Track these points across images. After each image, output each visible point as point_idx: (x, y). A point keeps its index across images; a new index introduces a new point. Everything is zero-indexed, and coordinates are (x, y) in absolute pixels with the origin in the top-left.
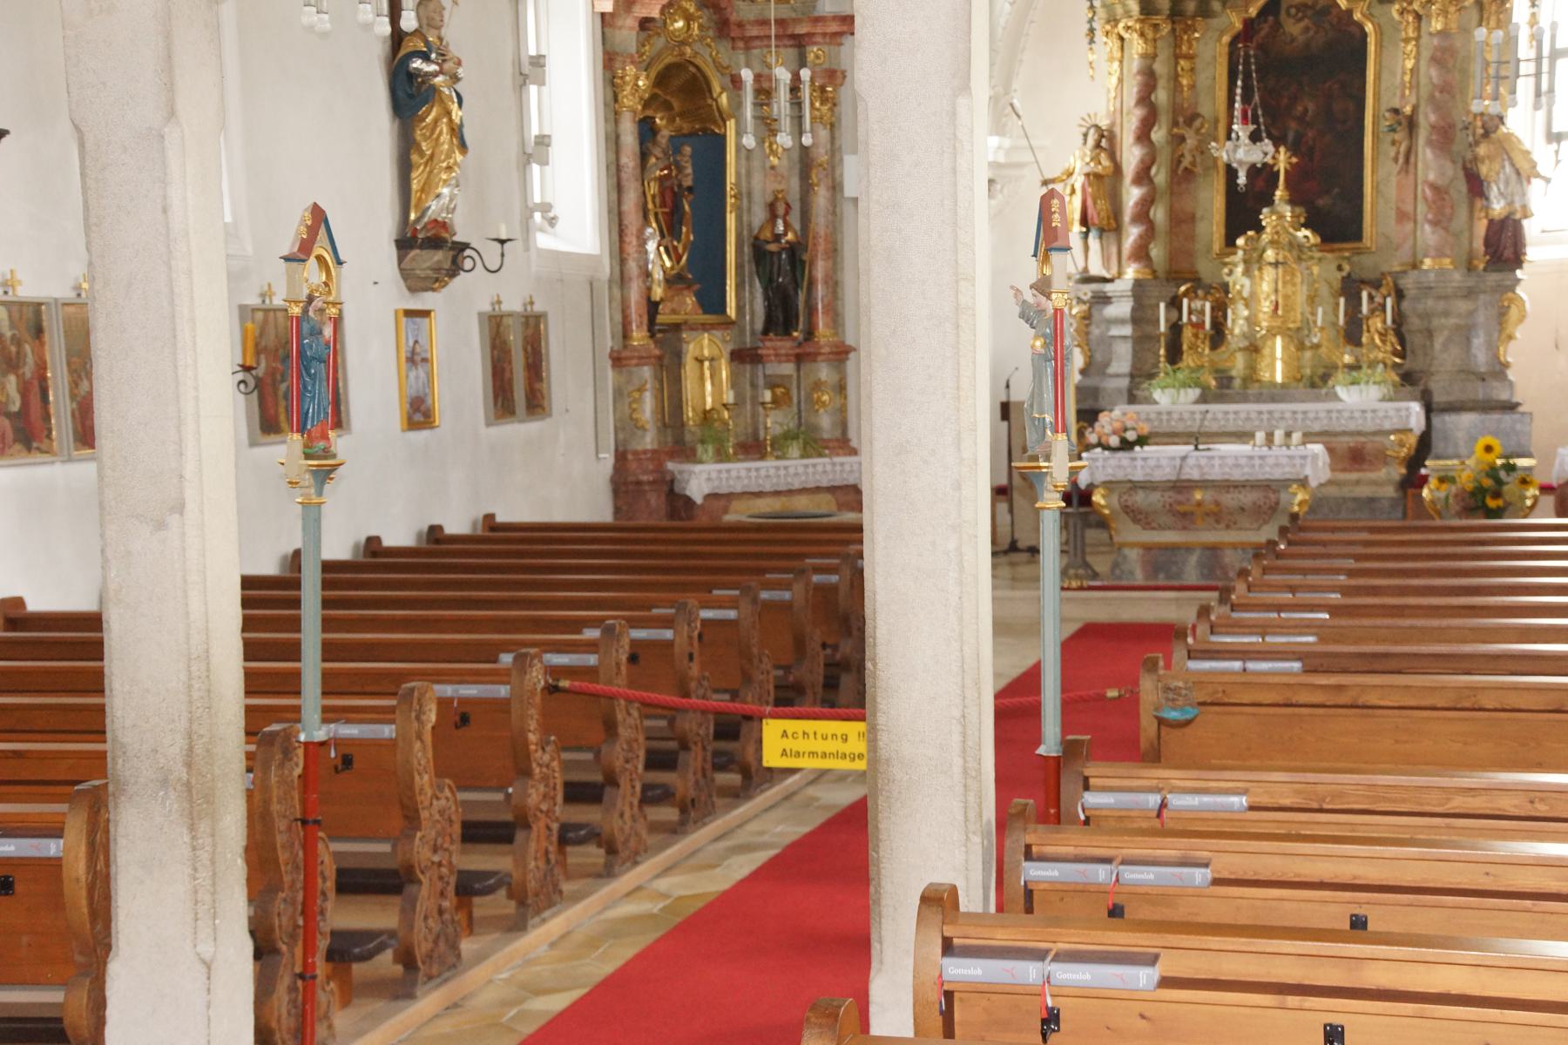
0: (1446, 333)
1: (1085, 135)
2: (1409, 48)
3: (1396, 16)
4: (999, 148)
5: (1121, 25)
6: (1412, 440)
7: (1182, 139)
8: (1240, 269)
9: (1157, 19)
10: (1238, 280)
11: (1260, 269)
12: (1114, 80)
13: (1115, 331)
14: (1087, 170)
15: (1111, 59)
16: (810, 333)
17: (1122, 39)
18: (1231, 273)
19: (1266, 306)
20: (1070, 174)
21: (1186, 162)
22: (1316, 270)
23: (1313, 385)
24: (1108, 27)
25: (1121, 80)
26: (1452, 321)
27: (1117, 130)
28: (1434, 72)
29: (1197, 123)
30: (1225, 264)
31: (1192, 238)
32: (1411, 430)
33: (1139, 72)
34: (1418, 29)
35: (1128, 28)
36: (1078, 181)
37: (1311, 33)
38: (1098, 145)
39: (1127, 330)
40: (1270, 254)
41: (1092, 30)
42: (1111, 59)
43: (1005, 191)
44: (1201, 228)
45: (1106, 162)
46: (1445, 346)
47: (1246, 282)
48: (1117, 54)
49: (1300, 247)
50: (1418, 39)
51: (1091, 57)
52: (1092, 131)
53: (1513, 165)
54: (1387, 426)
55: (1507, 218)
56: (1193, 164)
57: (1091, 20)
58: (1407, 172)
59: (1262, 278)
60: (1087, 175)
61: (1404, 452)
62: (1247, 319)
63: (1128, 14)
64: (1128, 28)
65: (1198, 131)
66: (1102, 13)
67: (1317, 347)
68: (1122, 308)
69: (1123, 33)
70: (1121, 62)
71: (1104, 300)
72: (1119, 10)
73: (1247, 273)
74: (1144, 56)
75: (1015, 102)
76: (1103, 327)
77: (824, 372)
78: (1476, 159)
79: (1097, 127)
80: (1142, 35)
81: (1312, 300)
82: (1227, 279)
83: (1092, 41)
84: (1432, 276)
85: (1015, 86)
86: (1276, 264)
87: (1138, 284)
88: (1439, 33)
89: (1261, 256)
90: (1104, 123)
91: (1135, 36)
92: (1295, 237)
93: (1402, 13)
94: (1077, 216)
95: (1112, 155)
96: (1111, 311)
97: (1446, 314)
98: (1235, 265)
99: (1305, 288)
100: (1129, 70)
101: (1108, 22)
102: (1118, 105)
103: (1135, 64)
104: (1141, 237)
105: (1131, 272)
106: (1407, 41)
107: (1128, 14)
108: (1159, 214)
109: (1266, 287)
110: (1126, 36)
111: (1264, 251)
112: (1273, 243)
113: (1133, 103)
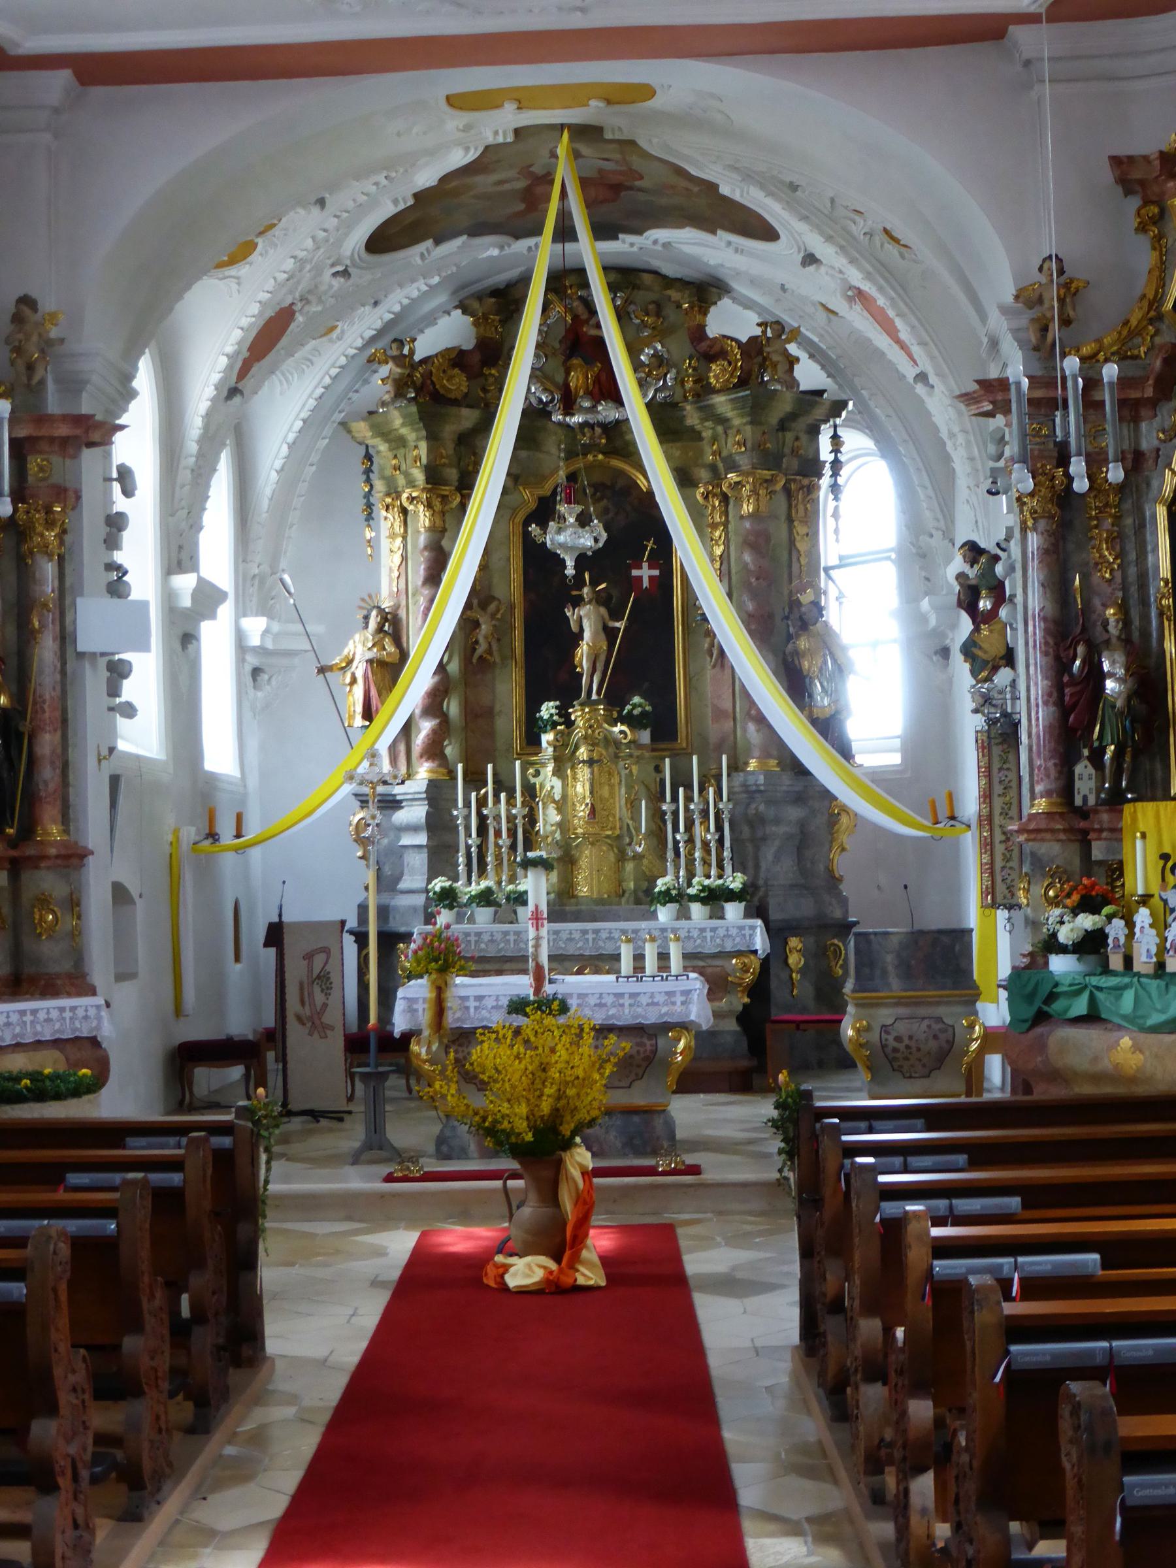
0: (777, 843)
1: (366, 618)
2: (717, 534)
3: (699, 497)
4: (266, 631)
5: (405, 496)
6: (755, 964)
7: (477, 624)
8: (550, 767)
9: (446, 490)
10: (548, 781)
11: (573, 768)
12: (397, 559)
13: (406, 840)
14: (369, 655)
15: (393, 536)
16: (28, 830)
17: (404, 511)
18: (537, 774)
19: (582, 811)
20: (350, 662)
21: (481, 649)
22: (635, 769)
23: (638, 902)
24: (389, 500)
25: (404, 558)
26: (782, 829)
27: (402, 613)
28: (747, 558)
29: (492, 607)
30: (533, 764)
31: (491, 734)
32: (755, 952)
33: (426, 548)
34: (726, 513)
35: (412, 499)
36: (359, 668)
37: (611, 515)
38: (380, 629)
39: (422, 839)
40: (583, 753)
41: (369, 506)
42: (393, 536)
43: (274, 682)
44: (500, 723)
45: (390, 648)
46: (777, 858)
47: (557, 783)
48: (399, 529)
49: (617, 744)
50: (726, 524)
51: (369, 534)
52: (374, 613)
53: (834, 660)
54: (729, 947)
55: (833, 716)
56: (489, 651)
57: (368, 495)
58: (722, 666)
59: (575, 779)
60: (370, 662)
61: (748, 978)
62: (560, 825)
63: (411, 483)
64: (412, 499)
65: (493, 616)
66: (379, 486)
67: (638, 857)
68: (415, 813)
69: (406, 504)
70: (404, 538)
71: (391, 804)
72: (401, 481)
73: (558, 772)
74: (432, 529)
75: (286, 577)
76: (392, 835)
77: (47, 882)
78: (796, 653)
79: (379, 607)
80: (429, 506)
81: (633, 805)
82: (533, 780)
83: (369, 517)
84: (761, 779)
85: (283, 564)
86: (590, 762)
87: (432, 784)
88: (750, 515)
89: (574, 752)
90: (386, 604)
91: (421, 508)
92: (611, 732)
93: (706, 498)
94: (359, 708)
95: (397, 639)
96: (400, 817)
97: (777, 821)
98: (544, 765)
99: (623, 790)
100: (415, 546)
101: (388, 495)
102: (402, 586)
103: (422, 540)
104: (434, 732)
105: (424, 771)
106: (714, 526)
107: (411, 483)
108: (453, 708)
109: (581, 788)
110: (411, 508)
111: (577, 748)
112: (585, 737)
113: (420, 583)
